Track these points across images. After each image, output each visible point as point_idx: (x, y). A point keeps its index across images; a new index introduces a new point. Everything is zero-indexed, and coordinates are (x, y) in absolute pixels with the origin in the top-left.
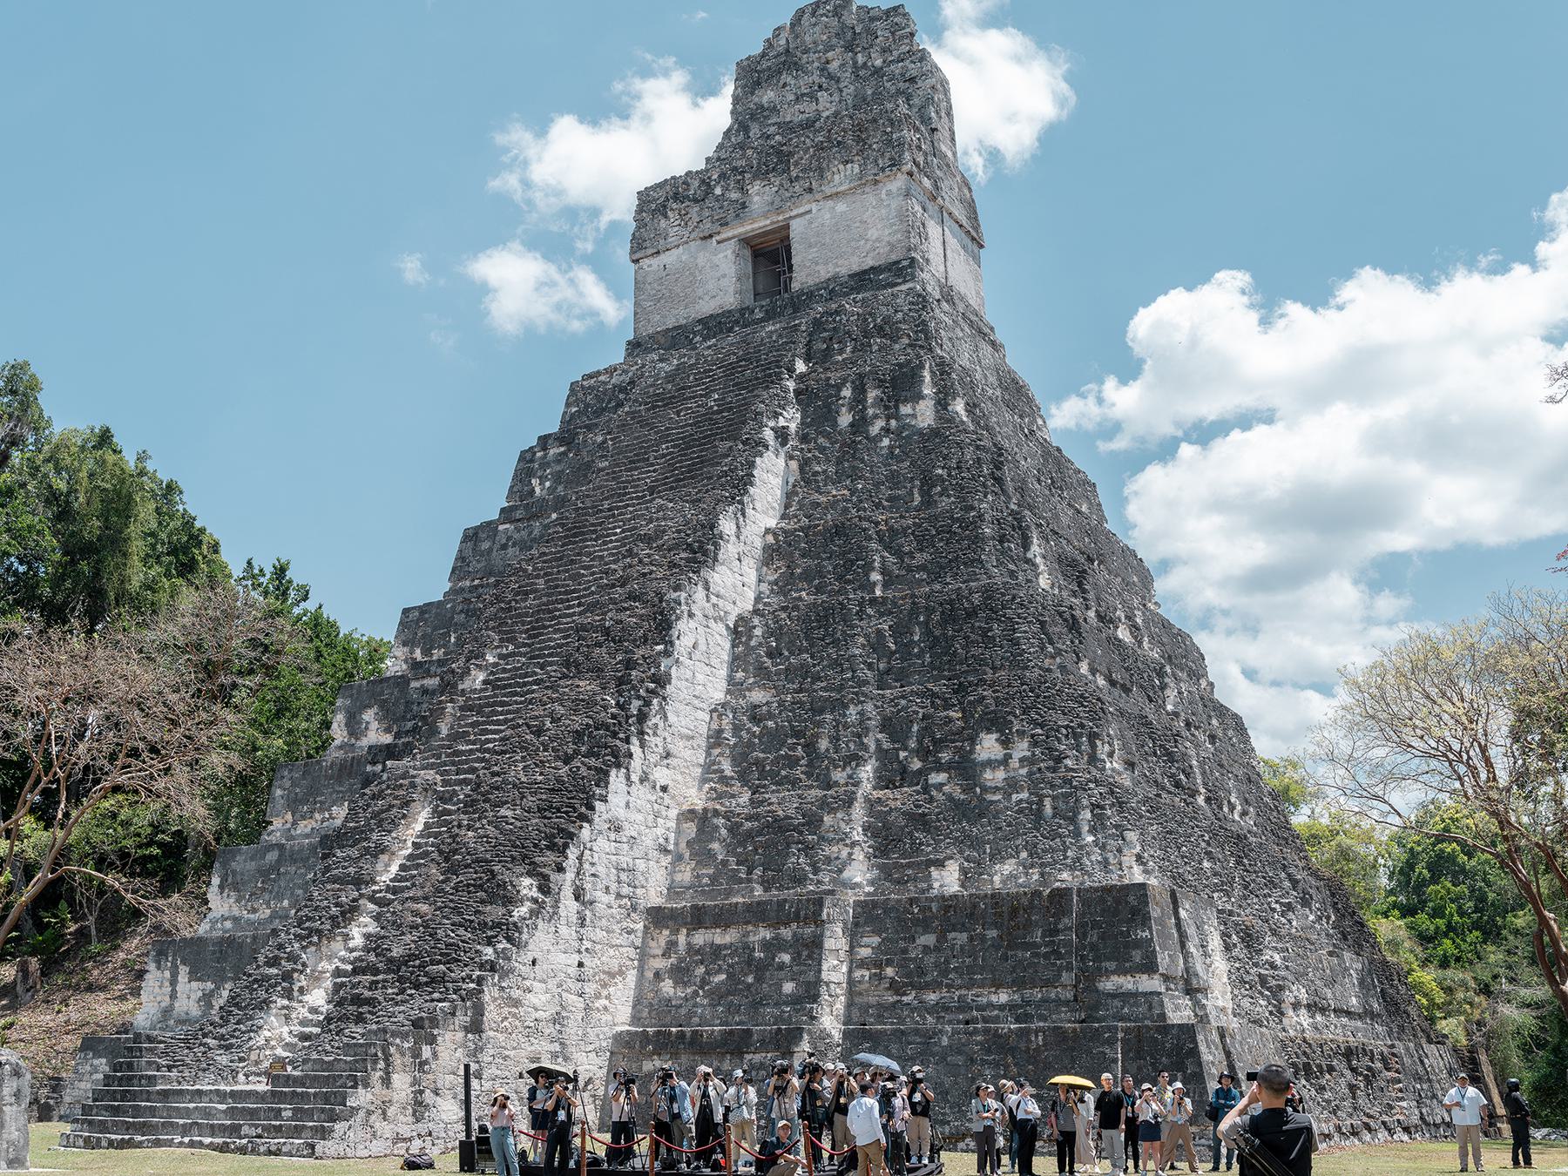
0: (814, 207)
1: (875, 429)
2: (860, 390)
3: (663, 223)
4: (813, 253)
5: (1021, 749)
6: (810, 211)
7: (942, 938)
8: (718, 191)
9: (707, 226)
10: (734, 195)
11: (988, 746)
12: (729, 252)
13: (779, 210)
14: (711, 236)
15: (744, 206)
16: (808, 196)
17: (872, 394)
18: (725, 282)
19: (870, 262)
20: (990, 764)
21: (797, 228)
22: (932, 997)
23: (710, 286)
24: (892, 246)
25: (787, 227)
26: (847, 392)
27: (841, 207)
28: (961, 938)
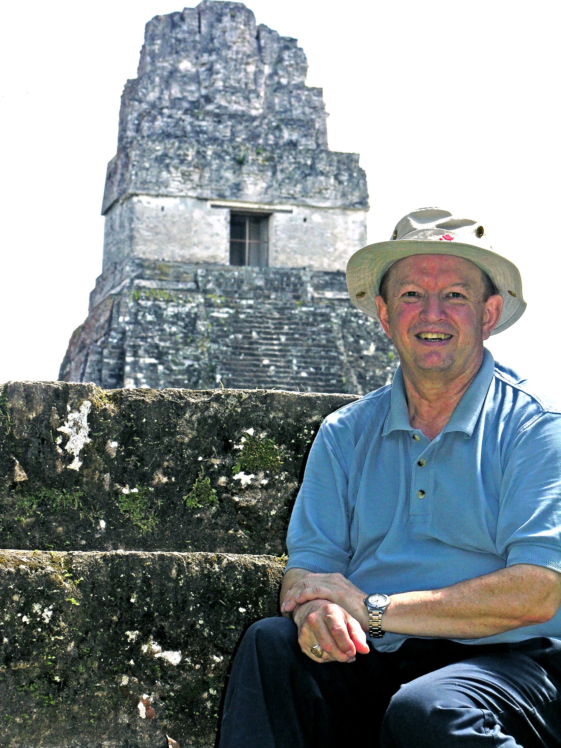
0: (295, 209)
3: (165, 174)
4: (293, 244)
6: (291, 212)
8: (214, 167)
9: (207, 193)
10: (228, 175)
12: (222, 218)
13: (270, 203)
14: (206, 200)
15: (238, 188)
16: (292, 201)
18: (217, 239)
21: (279, 220)
23: (206, 238)
27: (317, 218)
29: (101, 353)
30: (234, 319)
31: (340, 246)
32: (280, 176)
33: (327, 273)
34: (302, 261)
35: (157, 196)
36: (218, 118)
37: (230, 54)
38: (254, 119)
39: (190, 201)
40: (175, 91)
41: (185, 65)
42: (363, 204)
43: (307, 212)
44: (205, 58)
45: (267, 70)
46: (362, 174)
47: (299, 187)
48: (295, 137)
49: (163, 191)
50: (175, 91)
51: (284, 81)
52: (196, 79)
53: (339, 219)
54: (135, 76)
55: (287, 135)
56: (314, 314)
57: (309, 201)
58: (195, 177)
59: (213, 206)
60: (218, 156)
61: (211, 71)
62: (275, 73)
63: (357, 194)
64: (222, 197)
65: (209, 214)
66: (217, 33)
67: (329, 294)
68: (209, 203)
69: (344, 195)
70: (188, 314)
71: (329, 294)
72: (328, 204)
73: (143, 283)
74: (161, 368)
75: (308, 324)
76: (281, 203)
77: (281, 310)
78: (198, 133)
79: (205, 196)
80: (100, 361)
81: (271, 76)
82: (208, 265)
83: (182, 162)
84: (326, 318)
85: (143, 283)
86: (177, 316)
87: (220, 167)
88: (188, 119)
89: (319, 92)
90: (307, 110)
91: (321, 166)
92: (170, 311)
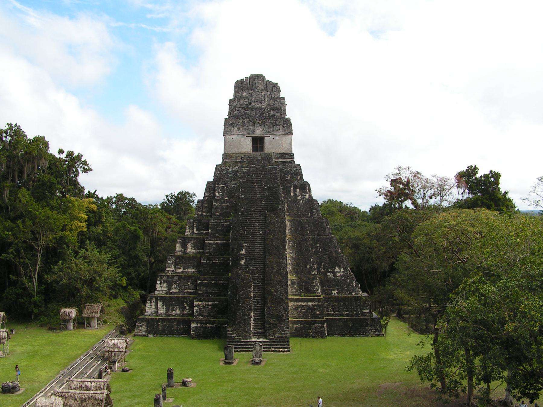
1: (299, 198)
4: (270, 146)
5: (342, 270)
7: (338, 303)
10: (251, 127)
11: (337, 269)
15: (254, 131)
17: (298, 190)
19: (283, 151)
20: (337, 272)
21: (266, 139)
22: (337, 313)
25: (263, 138)
26: (292, 188)
27: (277, 138)
28: (342, 303)
30: (248, 171)
31: (284, 146)
32: (266, 127)
34: (273, 151)
36: (252, 109)
37: (257, 90)
38: (263, 108)
40: (242, 102)
41: (245, 94)
42: (291, 133)
43: (274, 136)
44: (250, 92)
45: (268, 93)
47: (272, 130)
48: (275, 113)
49: (232, 133)
50: (242, 102)
51: (273, 96)
52: (247, 98)
53: (284, 138)
54: (232, 97)
55: (272, 112)
56: (272, 168)
58: (241, 129)
60: (248, 122)
63: (289, 130)
64: (249, 134)
65: (246, 139)
66: (254, 84)
67: (280, 160)
69: (285, 131)
70: (235, 171)
71: (280, 160)
73: (227, 160)
75: (271, 171)
77: (262, 167)
78: (246, 114)
81: (269, 95)
82: (245, 154)
83: (237, 125)
84: (276, 169)
85: (227, 160)
86: (232, 171)
87: (249, 125)
88: (243, 110)
90: (280, 104)
91: (278, 123)
92: (230, 170)
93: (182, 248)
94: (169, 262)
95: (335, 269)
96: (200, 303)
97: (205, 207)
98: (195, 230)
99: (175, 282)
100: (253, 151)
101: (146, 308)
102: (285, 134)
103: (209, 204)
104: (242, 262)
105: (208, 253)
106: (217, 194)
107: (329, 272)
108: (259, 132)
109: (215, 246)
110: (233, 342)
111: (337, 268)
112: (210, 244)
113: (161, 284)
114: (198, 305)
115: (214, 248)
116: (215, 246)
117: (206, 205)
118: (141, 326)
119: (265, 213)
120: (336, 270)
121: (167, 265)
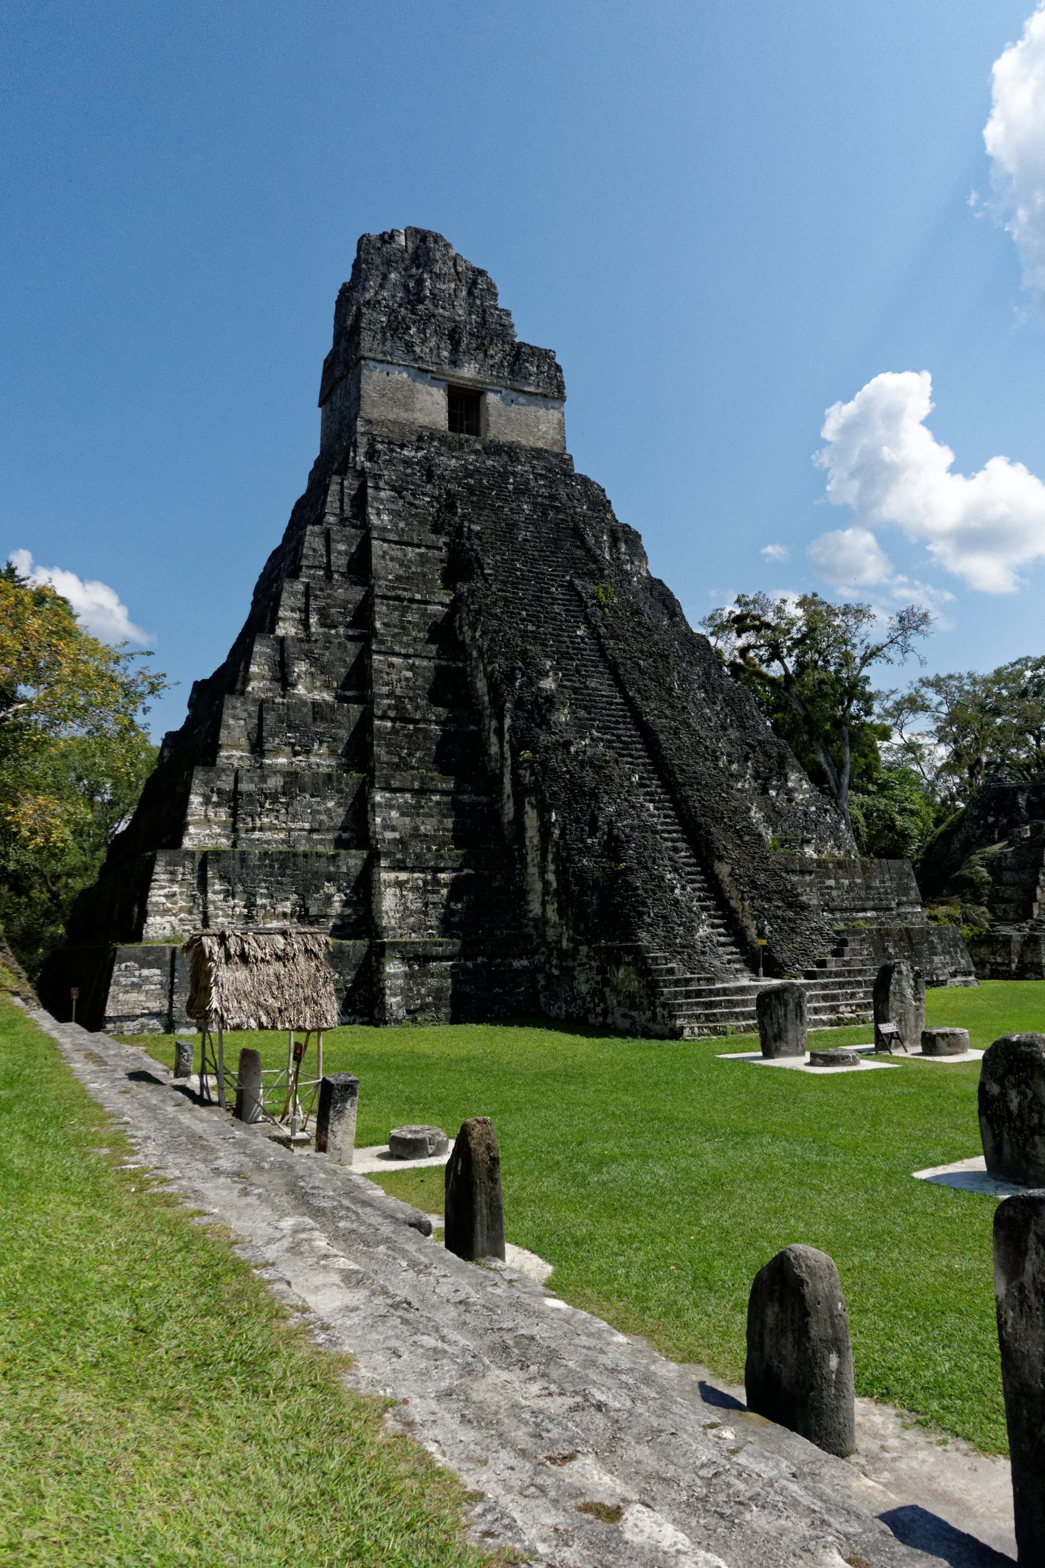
2: (615, 541)
4: (502, 421)
7: (837, 882)
15: (454, 363)
19: (540, 444)
24: (555, 442)
29: (342, 484)
33: (532, 449)
35: (382, 362)
39: (412, 370)
46: (558, 368)
57: (517, 385)
59: (433, 378)
61: (420, 282)
62: (470, 293)
68: (429, 375)
72: (532, 389)
74: (401, 502)
76: (492, 384)
79: (425, 366)
80: (342, 491)
89: (508, 314)
93: (274, 679)
94: (232, 722)
95: (786, 780)
96: (403, 876)
97: (340, 553)
98: (313, 620)
99: (274, 797)
100: (451, 429)
101: (150, 908)
102: (545, 396)
103: (350, 545)
104: (563, 716)
105: (388, 696)
106: (374, 519)
107: (774, 788)
108: (468, 372)
109: (409, 674)
110: (688, 995)
111: (793, 776)
112: (391, 665)
113: (207, 801)
114: (400, 884)
115: (407, 679)
116: (409, 674)
117: (342, 547)
118: (136, 987)
119: (571, 582)
120: (790, 784)
121: (223, 733)
